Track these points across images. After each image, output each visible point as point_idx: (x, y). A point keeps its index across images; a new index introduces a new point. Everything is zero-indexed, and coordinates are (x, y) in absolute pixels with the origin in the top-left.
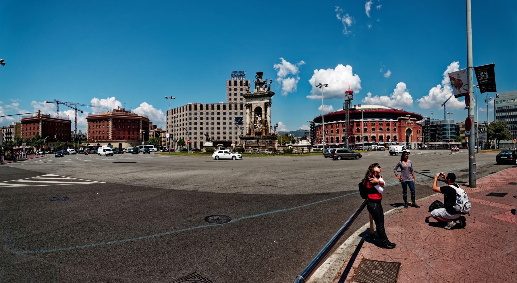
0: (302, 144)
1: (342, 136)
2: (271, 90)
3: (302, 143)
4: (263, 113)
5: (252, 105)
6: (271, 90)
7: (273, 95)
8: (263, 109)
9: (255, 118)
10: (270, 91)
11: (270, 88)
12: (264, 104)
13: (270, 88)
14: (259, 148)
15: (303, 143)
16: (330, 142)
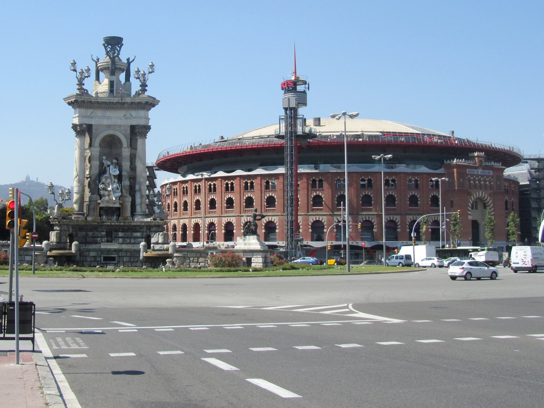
0: (245, 244)
1: (244, 220)
2: (150, 92)
3: (246, 242)
4: (126, 152)
5: (94, 128)
6: (150, 92)
7: (154, 106)
8: (125, 142)
9: (101, 164)
10: (147, 93)
11: (147, 86)
12: (129, 129)
13: (147, 86)
14: (120, 254)
15: (249, 244)
16: (223, 236)
